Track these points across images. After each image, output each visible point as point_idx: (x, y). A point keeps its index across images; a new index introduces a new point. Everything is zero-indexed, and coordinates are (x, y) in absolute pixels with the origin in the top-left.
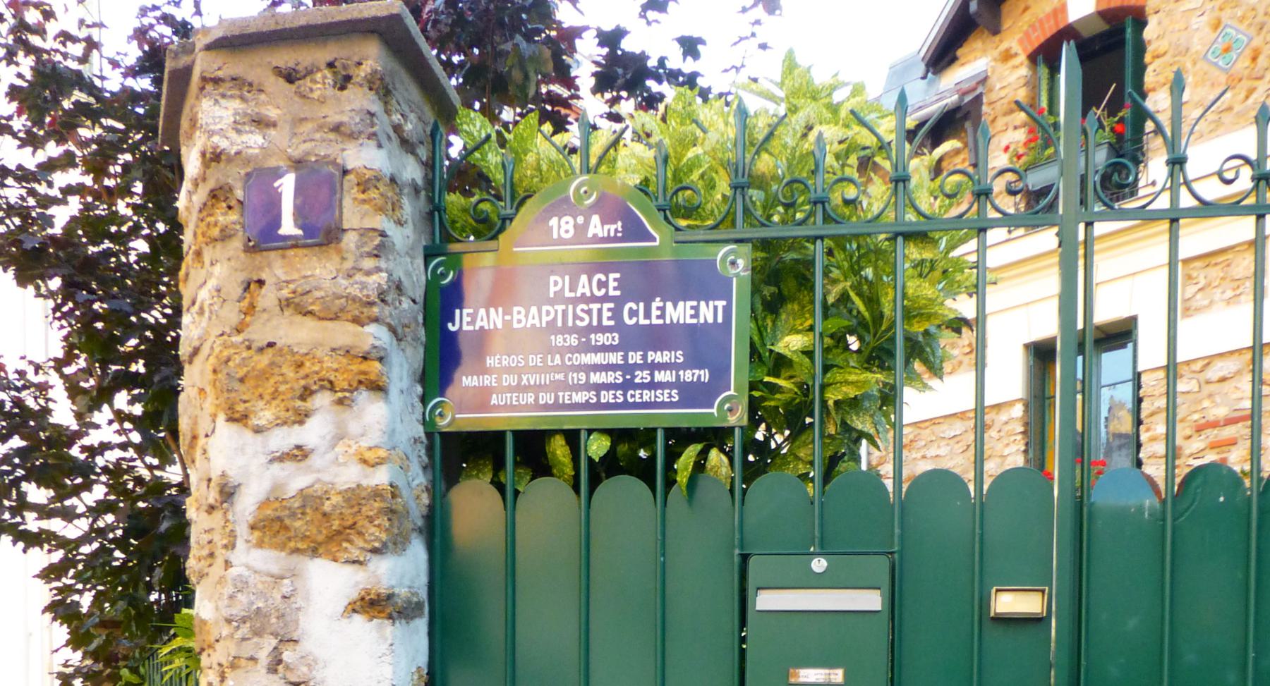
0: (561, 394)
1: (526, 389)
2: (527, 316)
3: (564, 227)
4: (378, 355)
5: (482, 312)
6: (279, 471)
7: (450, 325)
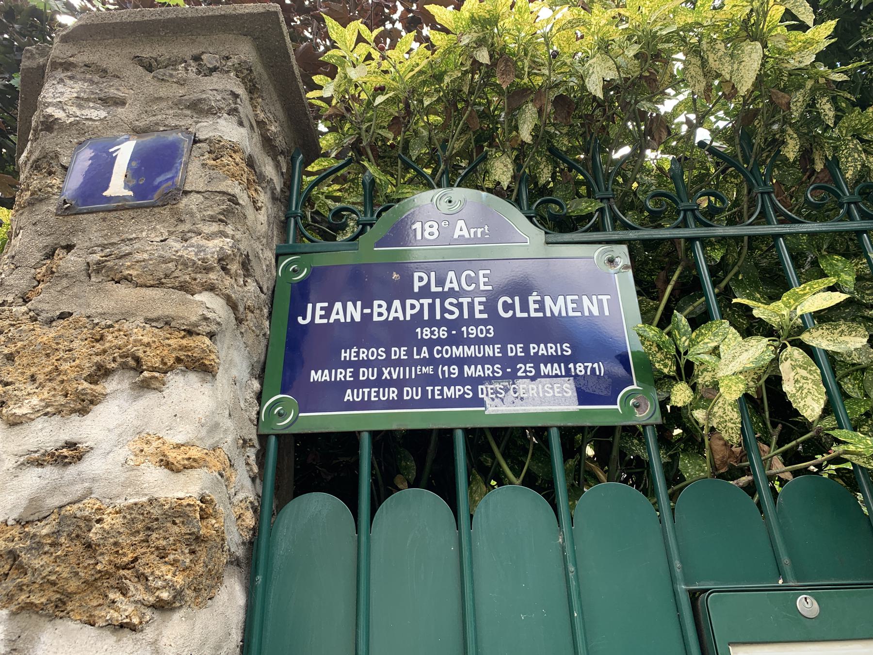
0: (429, 388)
1: (389, 383)
2: (389, 310)
3: (428, 230)
4: (208, 329)
6: (33, 480)
7: (300, 319)
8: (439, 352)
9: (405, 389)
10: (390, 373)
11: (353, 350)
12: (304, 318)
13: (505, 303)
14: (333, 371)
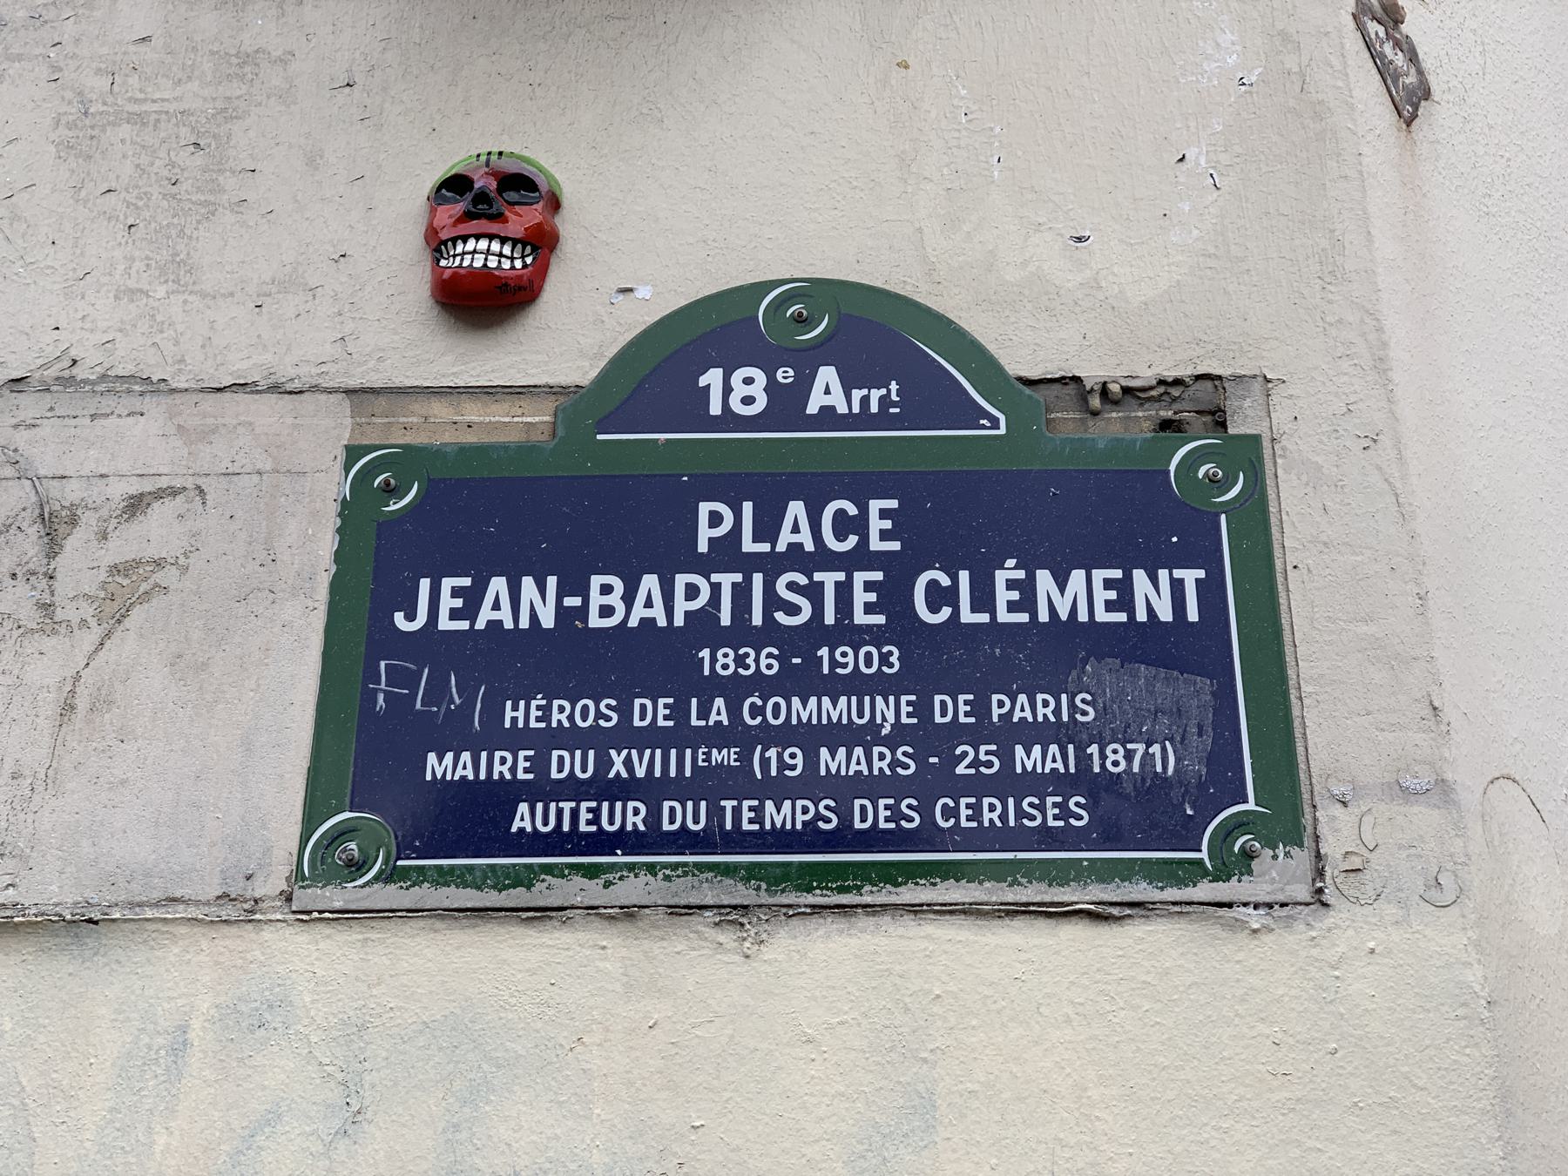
0: (728, 804)
2: (629, 598)
3: (740, 390)
5: (498, 585)
7: (399, 619)
8: (756, 711)
9: (666, 805)
10: (628, 763)
11: (534, 703)
12: (411, 617)
13: (933, 585)
14: (484, 755)
